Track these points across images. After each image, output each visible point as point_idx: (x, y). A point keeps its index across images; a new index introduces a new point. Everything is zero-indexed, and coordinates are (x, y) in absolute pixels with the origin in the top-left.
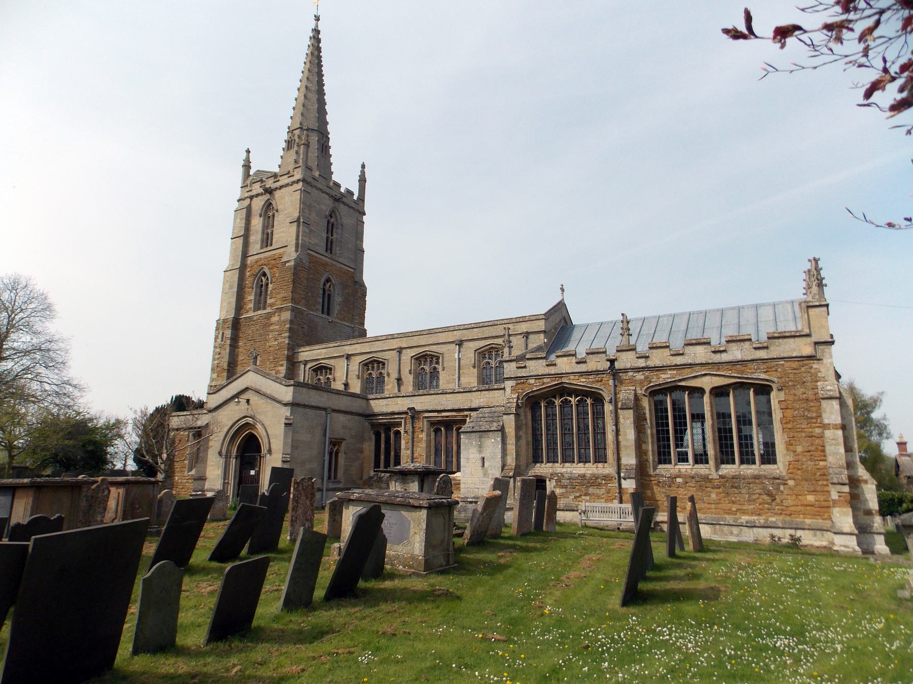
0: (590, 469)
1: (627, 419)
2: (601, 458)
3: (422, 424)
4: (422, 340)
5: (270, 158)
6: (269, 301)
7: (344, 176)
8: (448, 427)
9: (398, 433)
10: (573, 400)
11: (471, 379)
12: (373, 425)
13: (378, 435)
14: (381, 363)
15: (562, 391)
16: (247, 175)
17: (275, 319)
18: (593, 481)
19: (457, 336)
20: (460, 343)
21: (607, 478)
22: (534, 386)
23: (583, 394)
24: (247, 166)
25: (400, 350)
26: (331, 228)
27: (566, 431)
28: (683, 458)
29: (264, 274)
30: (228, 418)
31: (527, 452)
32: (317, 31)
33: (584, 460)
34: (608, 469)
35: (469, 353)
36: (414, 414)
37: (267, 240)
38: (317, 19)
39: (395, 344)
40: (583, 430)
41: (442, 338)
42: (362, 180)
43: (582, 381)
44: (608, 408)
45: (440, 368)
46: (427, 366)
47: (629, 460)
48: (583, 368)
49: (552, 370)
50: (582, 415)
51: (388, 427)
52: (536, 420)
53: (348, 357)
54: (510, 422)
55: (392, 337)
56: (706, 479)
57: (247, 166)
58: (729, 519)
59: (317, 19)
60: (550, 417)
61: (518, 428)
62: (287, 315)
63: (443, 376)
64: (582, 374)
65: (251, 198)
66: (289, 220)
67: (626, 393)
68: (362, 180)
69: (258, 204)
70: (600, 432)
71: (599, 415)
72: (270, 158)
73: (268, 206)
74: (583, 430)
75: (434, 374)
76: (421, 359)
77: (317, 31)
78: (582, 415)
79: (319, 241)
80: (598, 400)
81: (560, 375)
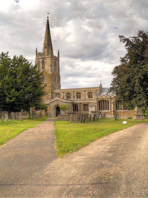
0: (107, 111)
1: (112, 105)
2: (108, 109)
3: (82, 105)
4: (78, 90)
5: (41, 50)
6: (45, 81)
7: (55, 54)
8: (86, 106)
9: (77, 106)
10: (105, 102)
11: (87, 97)
12: (73, 105)
13: (74, 106)
14: (69, 94)
15: (103, 100)
16: (37, 54)
17: (48, 84)
18: (108, 112)
19: (84, 90)
20: (85, 91)
21: (110, 112)
22: (99, 100)
23: (106, 101)
24: (37, 52)
25: (74, 92)
26: (55, 65)
27: (104, 105)
28: (119, 109)
29: (43, 75)
30: (53, 105)
31: (98, 109)
32: (48, 21)
33: (106, 110)
34: (110, 111)
35: (86, 93)
36: (81, 103)
37: (43, 68)
38: (48, 17)
39: (73, 90)
40: (106, 106)
41: (82, 90)
42: (59, 54)
43: (106, 99)
44: (110, 103)
45: (81, 95)
46: (79, 95)
47: (112, 110)
48: (106, 97)
49: (102, 98)
50: (106, 104)
51: (76, 105)
52: (99, 104)
53: (63, 92)
54: (96, 105)
55: (72, 89)
56: (122, 112)
57: (37, 52)
58: (124, 116)
59: (48, 17)
60: (102, 104)
61: (97, 105)
62: (50, 84)
63: (82, 97)
64: (106, 98)
65: (39, 59)
66: (49, 65)
67: (112, 101)
68: (59, 54)
69: (41, 60)
70: (108, 106)
71: (108, 104)
72: (41, 50)
73: (43, 61)
74: (106, 106)
75: (80, 96)
76: (77, 93)
77: (48, 21)
78: (106, 104)
79: (53, 69)
80: (108, 102)
81: (103, 98)
